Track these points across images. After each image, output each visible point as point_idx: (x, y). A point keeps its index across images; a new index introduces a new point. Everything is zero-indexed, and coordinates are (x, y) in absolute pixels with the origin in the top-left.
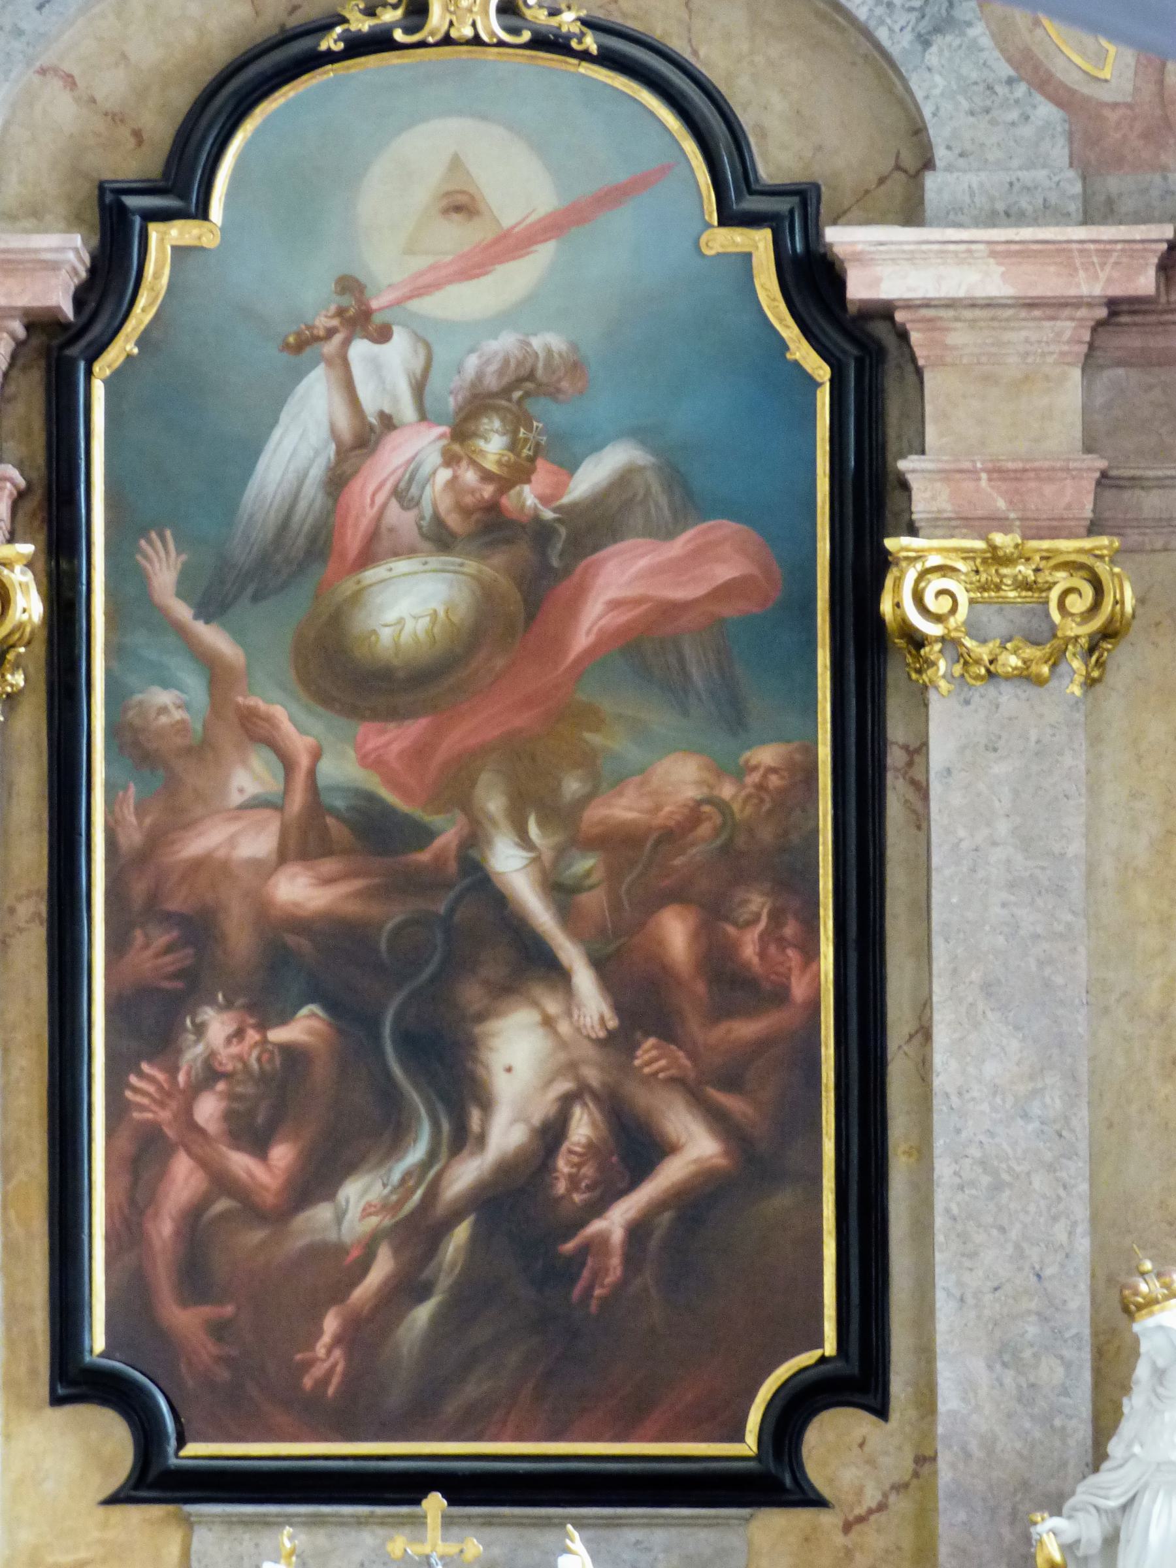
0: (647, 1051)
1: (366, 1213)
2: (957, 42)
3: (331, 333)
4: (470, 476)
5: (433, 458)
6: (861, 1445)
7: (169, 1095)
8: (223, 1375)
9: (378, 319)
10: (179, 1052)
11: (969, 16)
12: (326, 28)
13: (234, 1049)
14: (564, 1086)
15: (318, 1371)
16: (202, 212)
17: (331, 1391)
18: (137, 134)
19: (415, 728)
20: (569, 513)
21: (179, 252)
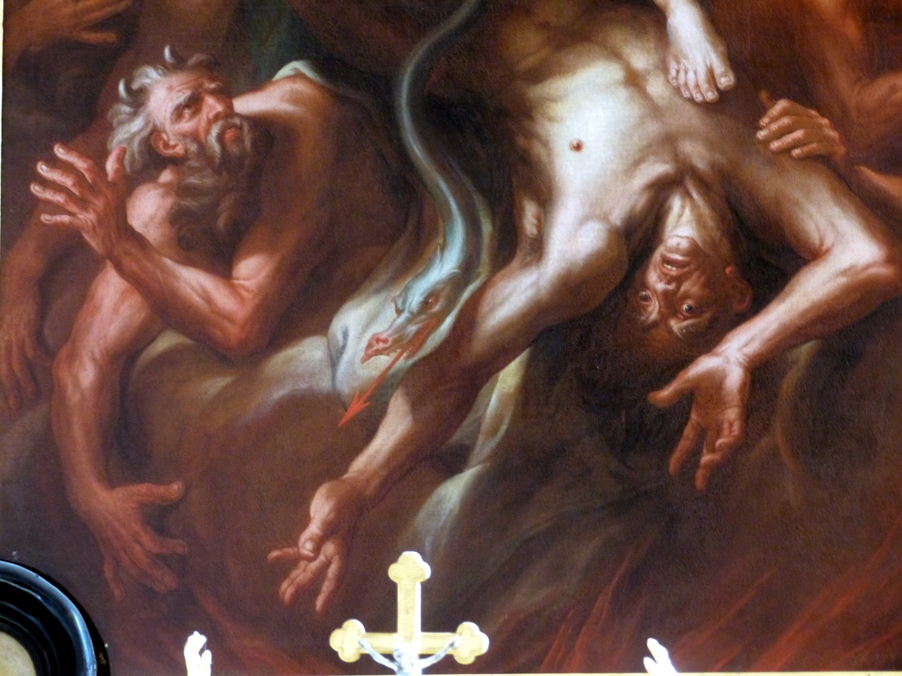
0: (774, 120)
1: (372, 351)
7: (93, 189)
8: (167, 580)
10: (109, 130)
13: (186, 125)
14: (657, 169)
15: (302, 574)
17: (319, 602)
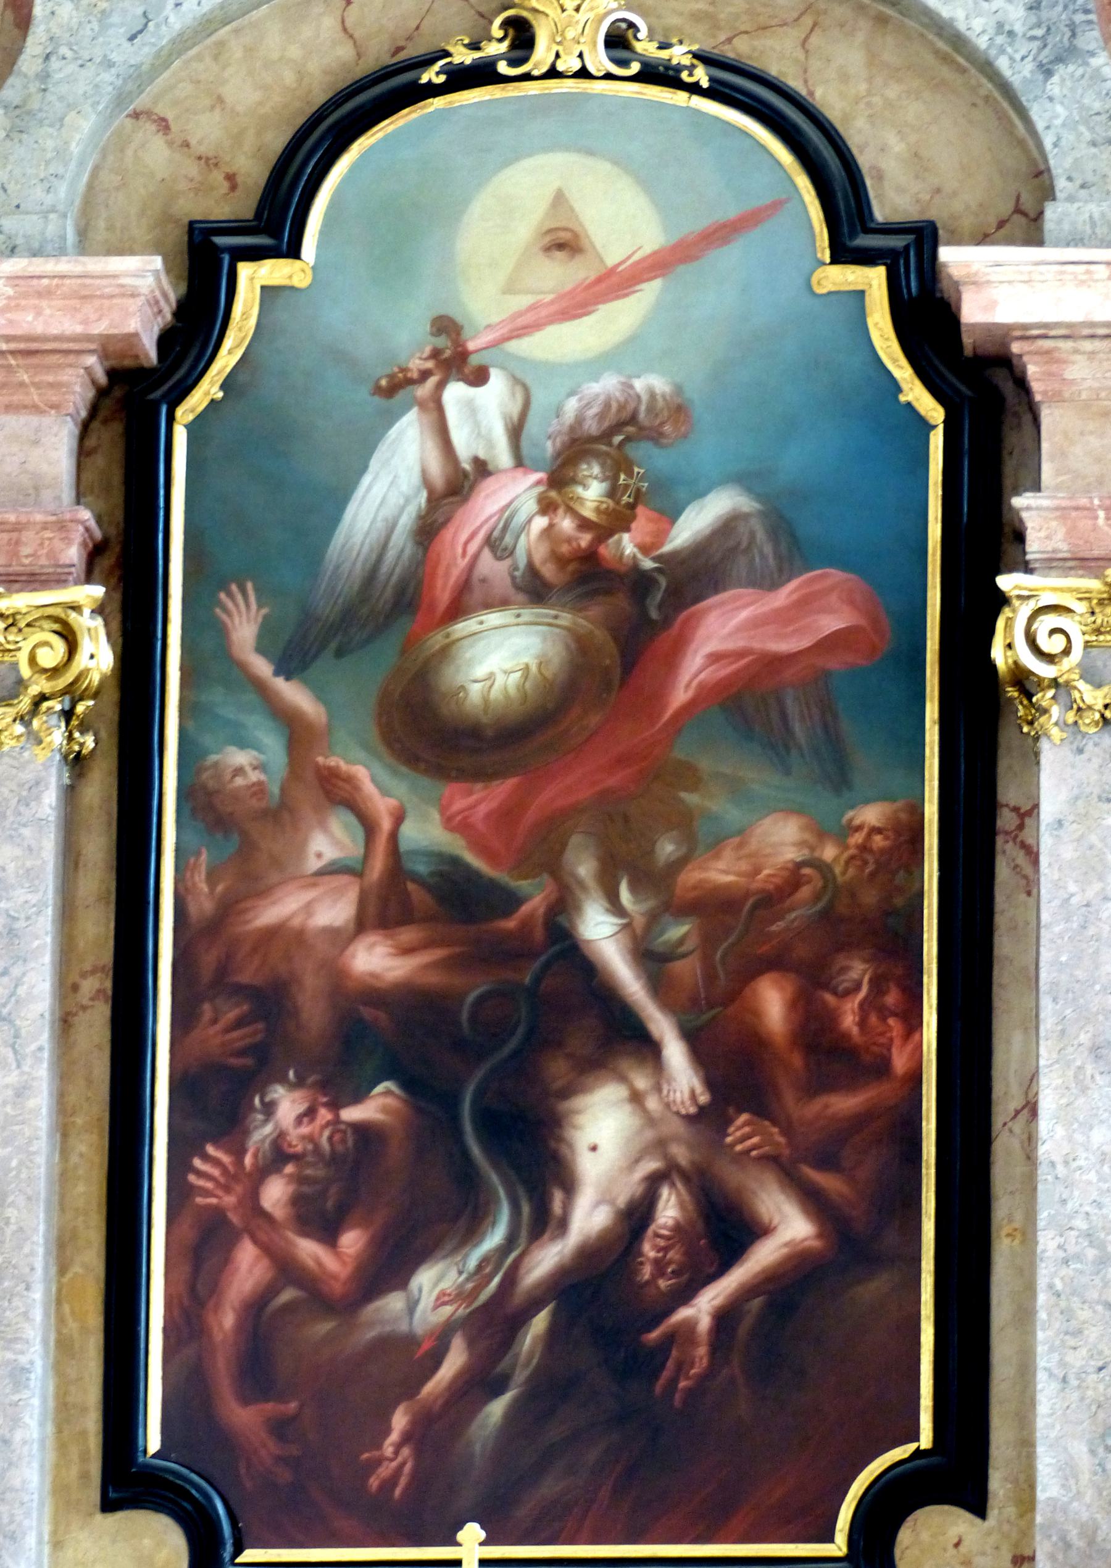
0: (739, 1128)
1: (440, 1302)
2: (1080, 71)
3: (425, 375)
4: (567, 524)
5: (528, 505)
6: (957, 1545)
7: (235, 1178)
8: (285, 1476)
9: (474, 360)
10: (246, 1133)
11: (1092, 46)
12: (427, 62)
13: (305, 1130)
14: (651, 1165)
16: (294, 252)
17: (398, 1492)
18: (231, 178)
19: (502, 790)
20: (669, 562)
21: (268, 293)
